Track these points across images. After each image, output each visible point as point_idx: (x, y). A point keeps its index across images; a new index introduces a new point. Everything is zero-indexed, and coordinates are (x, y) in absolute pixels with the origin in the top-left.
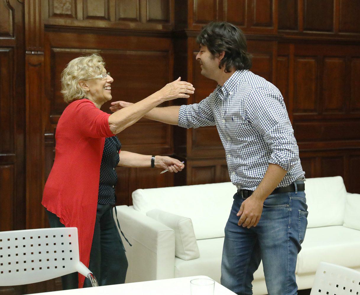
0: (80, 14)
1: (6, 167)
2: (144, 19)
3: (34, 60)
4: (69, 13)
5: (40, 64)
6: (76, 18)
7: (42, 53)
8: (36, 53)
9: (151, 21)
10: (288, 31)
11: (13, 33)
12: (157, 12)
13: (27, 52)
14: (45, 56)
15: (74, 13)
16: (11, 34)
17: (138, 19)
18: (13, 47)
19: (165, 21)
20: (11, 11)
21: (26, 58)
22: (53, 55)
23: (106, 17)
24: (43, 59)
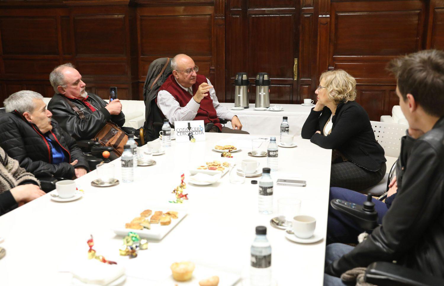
3: (324, 21)
5: (327, 23)
8: (325, 16)
11: (313, 5)
16: (312, 6)
18: (312, 14)
21: (319, 20)
22: (337, 17)
24: (329, 20)
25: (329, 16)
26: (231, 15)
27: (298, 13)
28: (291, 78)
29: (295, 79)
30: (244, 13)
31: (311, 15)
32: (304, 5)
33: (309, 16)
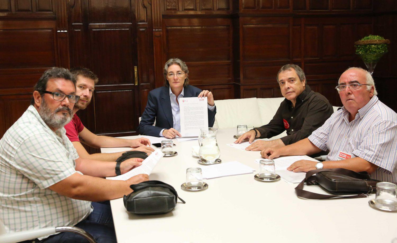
0: (180, 9)
1: (146, 90)
2: (215, 9)
3: (157, 34)
4: (175, 8)
5: (160, 36)
6: (179, 10)
7: (161, 30)
8: (158, 30)
9: (219, 9)
10: (300, 11)
11: (147, 21)
12: (223, 5)
13: (153, 30)
14: (163, 31)
15: (177, 8)
16: (146, 21)
17: (212, 9)
18: (147, 28)
19: (228, 9)
20: (145, 9)
22: (167, 31)
23: (195, 9)
25: (161, 30)
26: (72, 29)
27: (135, 27)
28: (132, 83)
29: (136, 85)
30: (86, 28)
31: (146, 29)
32: (139, 20)
33: (144, 30)
